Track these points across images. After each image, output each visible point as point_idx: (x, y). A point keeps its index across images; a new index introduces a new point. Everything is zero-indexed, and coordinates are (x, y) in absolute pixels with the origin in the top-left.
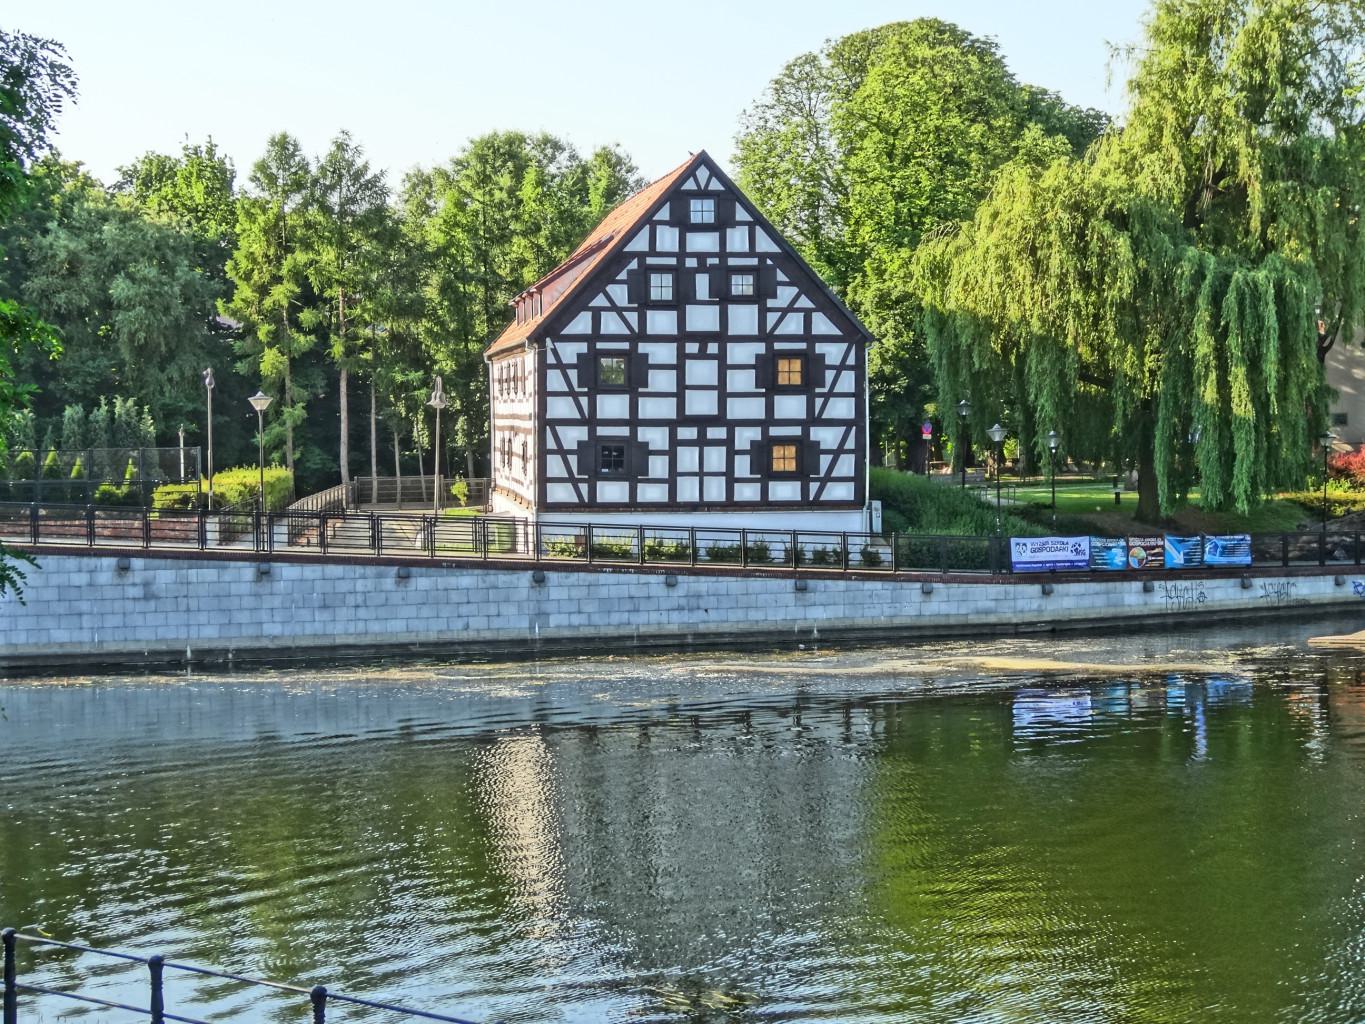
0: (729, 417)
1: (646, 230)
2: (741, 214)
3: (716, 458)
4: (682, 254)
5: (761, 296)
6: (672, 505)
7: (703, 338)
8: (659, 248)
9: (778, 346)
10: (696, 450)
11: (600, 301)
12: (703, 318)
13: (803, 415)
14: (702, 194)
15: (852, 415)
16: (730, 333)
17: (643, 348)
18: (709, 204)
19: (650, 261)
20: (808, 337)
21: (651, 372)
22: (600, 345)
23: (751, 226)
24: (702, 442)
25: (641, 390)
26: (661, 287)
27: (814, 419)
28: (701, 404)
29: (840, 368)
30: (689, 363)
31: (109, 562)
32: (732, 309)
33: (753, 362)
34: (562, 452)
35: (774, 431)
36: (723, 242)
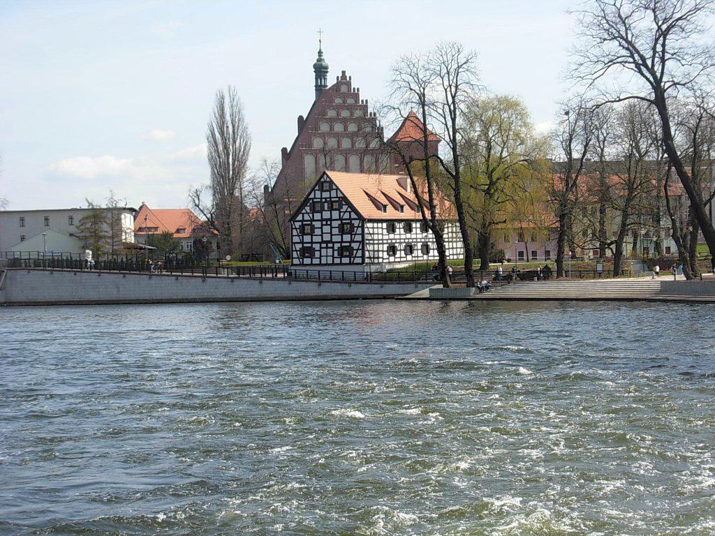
1: (313, 193)
3: (330, 251)
4: (321, 198)
6: (320, 264)
7: (327, 220)
9: (344, 221)
11: (304, 211)
14: (325, 182)
15: (360, 239)
17: (314, 223)
18: (328, 184)
19: (315, 200)
20: (350, 219)
22: (304, 223)
23: (336, 190)
24: (327, 248)
26: (318, 207)
27: (352, 241)
28: (326, 237)
30: (324, 227)
31: (174, 278)
32: (333, 212)
33: (337, 226)
34: (296, 251)
35: (343, 244)
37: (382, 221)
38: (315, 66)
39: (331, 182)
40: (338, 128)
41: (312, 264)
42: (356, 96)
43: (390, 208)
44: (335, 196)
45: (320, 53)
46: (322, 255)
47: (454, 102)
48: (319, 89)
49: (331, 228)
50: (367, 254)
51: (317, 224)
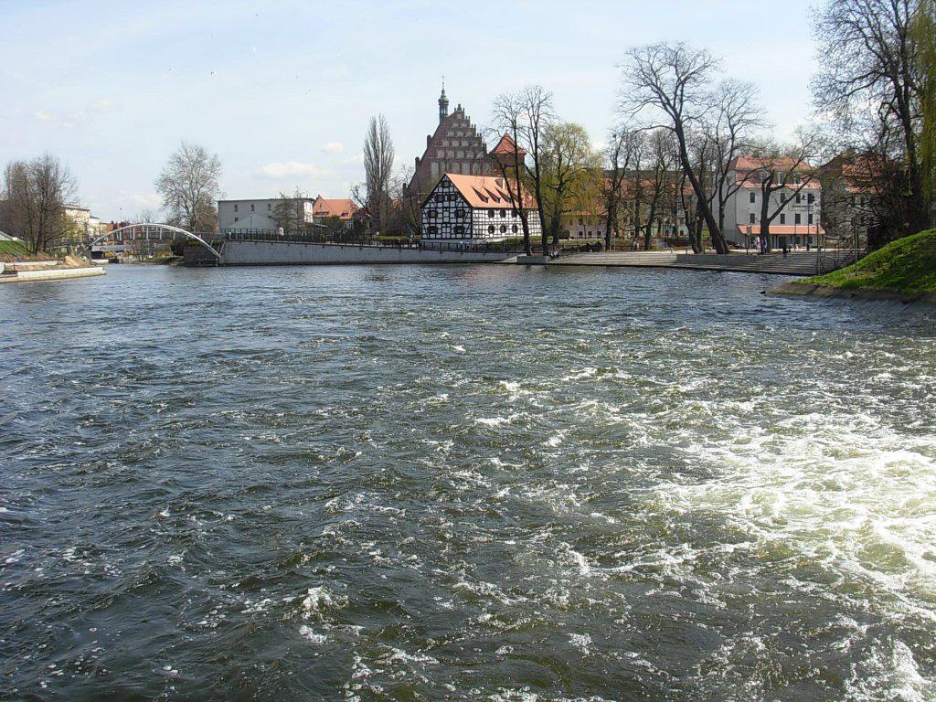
3: (448, 230)
5: (455, 200)
6: (442, 238)
12: (446, 204)
20: (463, 207)
24: (447, 227)
27: (464, 223)
28: (446, 220)
37: (485, 209)
38: (439, 101)
39: (450, 181)
40: (455, 144)
41: (436, 238)
42: (468, 122)
43: (490, 200)
45: (443, 92)
47: (536, 127)
48: (442, 116)
50: (474, 232)
51: (440, 211)
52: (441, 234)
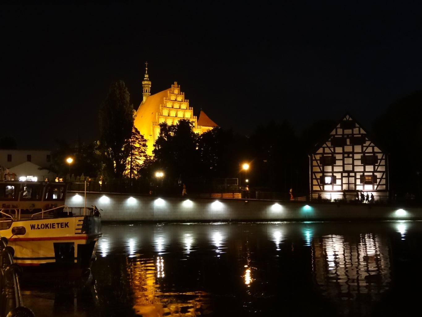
0: (355, 170)
2: (357, 125)
3: (352, 180)
4: (343, 134)
7: (348, 153)
8: (338, 133)
9: (366, 155)
10: (348, 178)
11: (325, 145)
12: (348, 149)
13: (372, 170)
16: (355, 151)
19: (336, 136)
20: (373, 152)
21: (337, 161)
22: (325, 155)
24: (349, 176)
25: (334, 165)
27: (375, 171)
29: (381, 160)
30: (345, 159)
32: (355, 146)
35: (366, 174)
36: (353, 131)
44: (358, 133)
46: (344, 182)
49: (353, 160)
52: (342, 185)
